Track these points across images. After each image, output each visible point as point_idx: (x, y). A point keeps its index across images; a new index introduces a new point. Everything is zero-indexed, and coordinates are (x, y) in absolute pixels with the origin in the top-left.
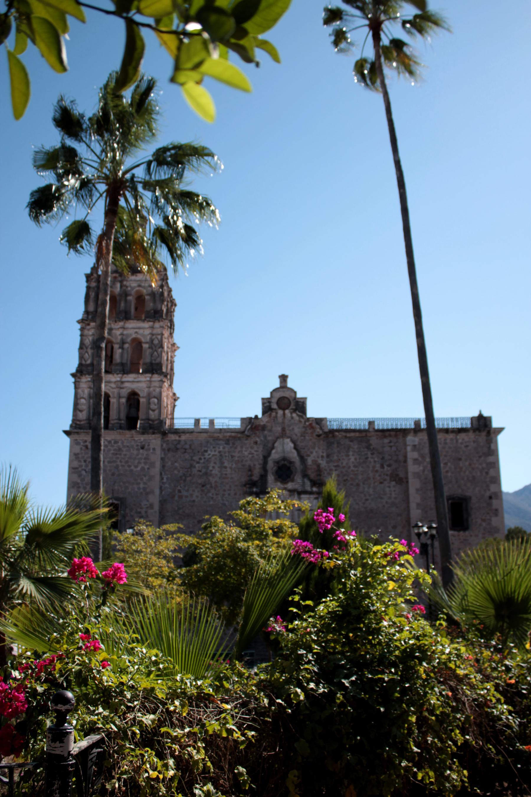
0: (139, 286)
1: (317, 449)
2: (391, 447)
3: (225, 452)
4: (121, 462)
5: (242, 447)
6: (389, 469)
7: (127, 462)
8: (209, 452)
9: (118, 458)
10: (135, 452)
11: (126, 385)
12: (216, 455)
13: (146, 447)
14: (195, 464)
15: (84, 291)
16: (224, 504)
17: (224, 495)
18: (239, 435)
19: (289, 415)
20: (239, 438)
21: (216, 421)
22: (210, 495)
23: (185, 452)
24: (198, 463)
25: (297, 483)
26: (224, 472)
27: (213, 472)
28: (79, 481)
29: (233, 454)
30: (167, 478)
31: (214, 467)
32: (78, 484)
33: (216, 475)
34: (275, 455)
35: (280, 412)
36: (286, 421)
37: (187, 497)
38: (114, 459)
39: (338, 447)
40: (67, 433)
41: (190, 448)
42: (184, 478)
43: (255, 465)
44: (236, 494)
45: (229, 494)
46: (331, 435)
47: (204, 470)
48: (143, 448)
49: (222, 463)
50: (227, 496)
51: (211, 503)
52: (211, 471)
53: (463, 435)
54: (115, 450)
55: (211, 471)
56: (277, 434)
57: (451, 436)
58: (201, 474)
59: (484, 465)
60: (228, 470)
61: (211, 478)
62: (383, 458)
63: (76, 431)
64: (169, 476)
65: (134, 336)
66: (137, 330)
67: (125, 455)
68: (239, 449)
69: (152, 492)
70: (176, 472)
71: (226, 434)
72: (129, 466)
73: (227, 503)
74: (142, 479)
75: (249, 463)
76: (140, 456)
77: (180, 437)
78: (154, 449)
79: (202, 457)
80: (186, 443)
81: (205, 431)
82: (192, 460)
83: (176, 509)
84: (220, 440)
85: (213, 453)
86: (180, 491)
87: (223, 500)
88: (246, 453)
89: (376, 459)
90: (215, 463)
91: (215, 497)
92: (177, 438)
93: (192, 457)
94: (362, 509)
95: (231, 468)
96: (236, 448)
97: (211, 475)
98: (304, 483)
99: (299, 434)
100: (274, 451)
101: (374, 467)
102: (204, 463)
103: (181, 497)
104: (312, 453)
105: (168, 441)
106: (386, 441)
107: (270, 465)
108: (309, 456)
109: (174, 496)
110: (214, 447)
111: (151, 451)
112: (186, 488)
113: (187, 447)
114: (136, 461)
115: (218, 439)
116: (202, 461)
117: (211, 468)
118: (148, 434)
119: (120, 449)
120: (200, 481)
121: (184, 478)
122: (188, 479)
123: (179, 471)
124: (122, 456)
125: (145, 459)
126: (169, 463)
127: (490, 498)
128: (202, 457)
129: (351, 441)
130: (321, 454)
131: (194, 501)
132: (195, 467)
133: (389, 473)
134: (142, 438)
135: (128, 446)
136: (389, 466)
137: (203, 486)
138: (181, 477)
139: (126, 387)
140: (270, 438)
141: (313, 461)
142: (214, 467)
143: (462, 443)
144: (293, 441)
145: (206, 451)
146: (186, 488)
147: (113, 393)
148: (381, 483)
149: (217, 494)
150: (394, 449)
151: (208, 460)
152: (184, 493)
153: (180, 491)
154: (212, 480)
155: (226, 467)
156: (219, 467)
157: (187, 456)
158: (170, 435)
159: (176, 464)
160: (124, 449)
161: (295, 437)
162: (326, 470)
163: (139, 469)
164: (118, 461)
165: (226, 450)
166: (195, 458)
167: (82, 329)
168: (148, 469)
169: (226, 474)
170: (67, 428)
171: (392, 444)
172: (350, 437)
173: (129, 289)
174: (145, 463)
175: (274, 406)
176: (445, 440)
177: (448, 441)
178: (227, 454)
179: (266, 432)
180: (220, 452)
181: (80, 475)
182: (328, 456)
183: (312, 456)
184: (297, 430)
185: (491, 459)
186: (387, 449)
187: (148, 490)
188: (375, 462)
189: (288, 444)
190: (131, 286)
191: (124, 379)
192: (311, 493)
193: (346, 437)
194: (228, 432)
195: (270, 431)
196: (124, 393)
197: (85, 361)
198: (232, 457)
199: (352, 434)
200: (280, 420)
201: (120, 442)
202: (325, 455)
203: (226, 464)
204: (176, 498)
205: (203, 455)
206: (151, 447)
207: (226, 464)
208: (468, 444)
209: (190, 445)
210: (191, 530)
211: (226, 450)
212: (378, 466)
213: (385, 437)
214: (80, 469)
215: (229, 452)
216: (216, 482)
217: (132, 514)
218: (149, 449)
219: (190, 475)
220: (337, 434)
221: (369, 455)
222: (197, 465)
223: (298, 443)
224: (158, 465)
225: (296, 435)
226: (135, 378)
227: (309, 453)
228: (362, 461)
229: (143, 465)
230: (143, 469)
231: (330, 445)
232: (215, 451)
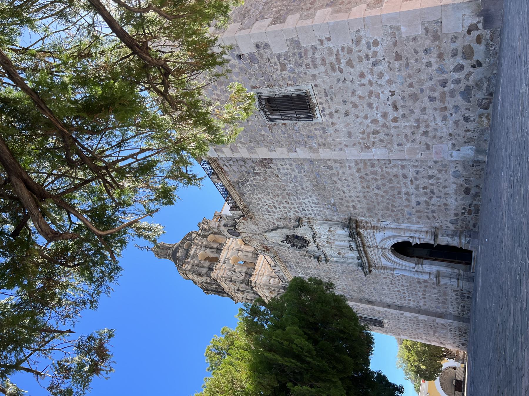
35: (243, 235)
46: (245, 209)
49: (305, 267)
88: (290, 256)
101: (263, 181)
104: (270, 221)
136: (254, 169)
162: (283, 214)
183: (273, 221)
212: (257, 177)
221: (250, 182)
228: (259, 189)
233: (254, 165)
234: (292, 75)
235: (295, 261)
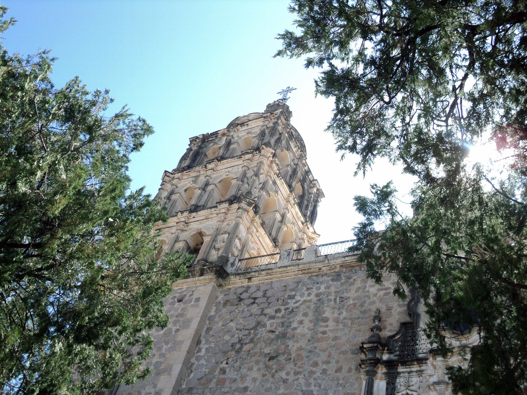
3: (329, 294)
8: (298, 298)
17: (312, 373)
22: (283, 374)
24: (272, 317)
27: (298, 331)
41: (264, 296)
43: (389, 309)
47: (280, 329)
52: (295, 329)
55: (295, 329)
60: (331, 324)
61: (290, 343)
65: (224, 176)
66: (229, 169)
69: (168, 370)
70: (227, 337)
71: (332, 262)
74: (160, 349)
75: (378, 305)
77: (250, 279)
78: (198, 300)
79: (283, 308)
86: (223, 371)
91: (291, 378)
92: (246, 283)
96: (352, 284)
110: (308, 289)
113: (260, 294)
115: (320, 273)
117: (295, 325)
118: (194, 276)
120: (267, 351)
121: (238, 346)
122: (246, 348)
126: (220, 324)
128: (283, 308)
132: (264, 326)
137: (271, 358)
138: (233, 345)
142: (301, 322)
149: (296, 373)
151: (292, 311)
154: (293, 346)
155: (326, 320)
156: (311, 321)
157: (255, 309)
159: (232, 324)
165: (333, 289)
166: (267, 311)
168: (177, 331)
169: (324, 333)
180: (317, 295)
194: (337, 258)
204: (212, 385)
205: (285, 303)
207: (326, 315)
211: (333, 289)
216: (300, 349)
219: (252, 341)
235: (352, 294)
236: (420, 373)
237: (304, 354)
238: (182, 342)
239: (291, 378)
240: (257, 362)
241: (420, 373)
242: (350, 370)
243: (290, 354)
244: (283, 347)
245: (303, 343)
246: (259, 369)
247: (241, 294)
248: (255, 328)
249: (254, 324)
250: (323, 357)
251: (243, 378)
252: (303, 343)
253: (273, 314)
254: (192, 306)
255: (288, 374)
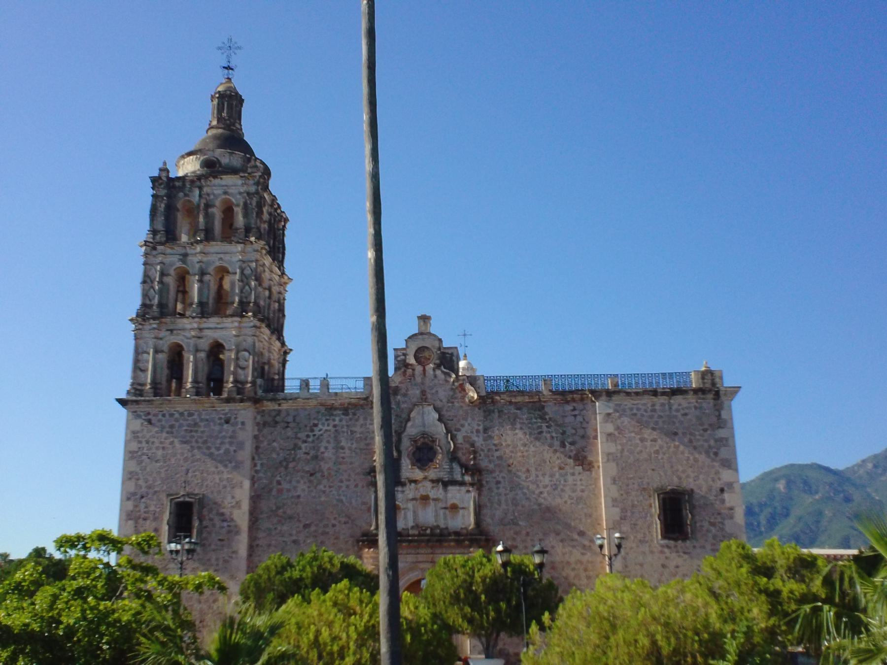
0: (225, 193)
1: (469, 420)
2: (575, 416)
3: (342, 427)
4: (197, 442)
5: (365, 419)
6: (573, 448)
7: (205, 442)
8: (320, 426)
9: (193, 437)
10: (217, 428)
11: (207, 333)
12: (330, 431)
13: (232, 421)
14: (300, 443)
15: (149, 201)
16: (341, 501)
17: (340, 487)
18: (362, 402)
19: (431, 372)
20: (362, 406)
21: (332, 382)
22: (321, 487)
23: (287, 427)
24: (305, 442)
25: (440, 467)
26: (342, 455)
27: (326, 455)
28: (138, 470)
29: (354, 429)
30: (262, 464)
31: (326, 448)
32: (137, 474)
33: (330, 459)
34: (412, 430)
36: (427, 381)
37: (289, 490)
38: (188, 438)
39: (499, 416)
40: (122, 402)
41: (294, 420)
42: (284, 464)
44: (356, 486)
45: (348, 487)
47: (312, 453)
48: (227, 422)
50: (344, 488)
51: (323, 499)
52: (323, 453)
53: (678, 400)
54: (189, 425)
55: (323, 453)
56: (415, 400)
57: (663, 399)
58: (308, 457)
59: (712, 443)
60: (347, 451)
61: (322, 463)
62: (564, 433)
63: (134, 398)
64: (265, 461)
65: (218, 264)
66: (222, 256)
67: (203, 432)
68: (361, 421)
70: (274, 456)
72: (209, 448)
73: (344, 498)
76: (224, 433)
77: (279, 405)
79: (311, 434)
80: (288, 415)
81: (315, 396)
82: (297, 438)
83: (274, 508)
84: (336, 409)
85: (326, 428)
86: (279, 483)
87: (339, 495)
89: (554, 435)
90: (328, 442)
91: (328, 490)
93: (296, 433)
94: (536, 507)
95: (350, 449)
96: (357, 420)
97: (323, 459)
98: (452, 468)
99: (445, 400)
100: (409, 424)
102: (313, 442)
103: (280, 491)
104: (463, 426)
105: (264, 411)
106: (568, 408)
107: (406, 444)
108: (458, 430)
109: (271, 490)
111: (240, 426)
112: (288, 478)
113: (290, 419)
114: (219, 441)
116: (310, 440)
117: (322, 449)
119: (196, 424)
120: (307, 468)
121: (284, 464)
122: (291, 465)
123: (278, 455)
124: (199, 434)
125: (231, 437)
126: (265, 443)
127: (722, 490)
129: (519, 409)
130: (476, 427)
131: (299, 497)
132: (300, 448)
133: (572, 454)
134: (227, 407)
135: (207, 420)
136: (572, 444)
137: (312, 475)
138: (281, 462)
139: (206, 336)
140: (404, 406)
141: (464, 437)
142: (326, 448)
143: (677, 410)
144: (436, 409)
145: (316, 425)
146: (288, 478)
147: (188, 344)
148: (561, 468)
149: (330, 487)
150: (579, 419)
151: (318, 438)
152: (285, 486)
153: (279, 483)
154: (325, 466)
155: (343, 448)
157: (290, 433)
158: (265, 403)
159: (275, 444)
160: (202, 424)
161: (439, 404)
162: (483, 450)
163: (222, 451)
164: (194, 440)
166: (300, 435)
167: (146, 254)
168: (235, 451)
169: (343, 458)
170: (123, 396)
171: (576, 412)
172: (516, 403)
173: (212, 197)
174: (231, 443)
175: (411, 360)
176: (653, 405)
177: (657, 407)
178: (345, 429)
179: (399, 397)
180: (335, 426)
181: (140, 463)
182: (486, 430)
183: (463, 430)
184: (443, 394)
185: (721, 433)
186: (569, 419)
187: (235, 481)
188: (552, 437)
189: (429, 413)
190: (214, 194)
191: (203, 326)
192: (462, 484)
193: (511, 403)
195: (405, 395)
196: (205, 344)
197: (150, 300)
198: (352, 432)
199: (519, 399)
200: (419, 379)
201: (196, 413)
202: (481, 428)
203: (343, 444)
204: (274, 493)
205: (312, 431)
206: (240, 420)
207: (343, 444)
208: (686, 411)
209: (294, 417)
210: (294, 538)
211: (344, 423)
213: (567, 402)
214: (139, 453)
215: (347, 426)
216: (329, 469)
217: (211, 516)
218: (237, 423)
219: (294, 460)
220: (498, 398)
221: (544, 429)
222: (303, 446)
223: (444, 412)
224: (249, 447)
225: (441, 401)
226: (218, 323)
227: (458, 426)
229: (227, 446)
230: (227, 452)
231: (488, 413)
232: (328, 425)
233: (578, 446)
234: (704, 529)
236: (403, 492)
237: (333, 473)
238: (242, 462)
239: (328, 490)
240: (302, 477)
241: (403, 492)
242: (363, 487)
243: (323, 472)
244: (317, 467)
245: (330, 464)
246: (305, 483)
247: (275, 417)
248: (294, 449)
249: (292, 446)
250: (345, 477)
251: (295, 488)
252: (330, 464)
253: (305, 438)
254: (240, 429)
255: (325, 487)
